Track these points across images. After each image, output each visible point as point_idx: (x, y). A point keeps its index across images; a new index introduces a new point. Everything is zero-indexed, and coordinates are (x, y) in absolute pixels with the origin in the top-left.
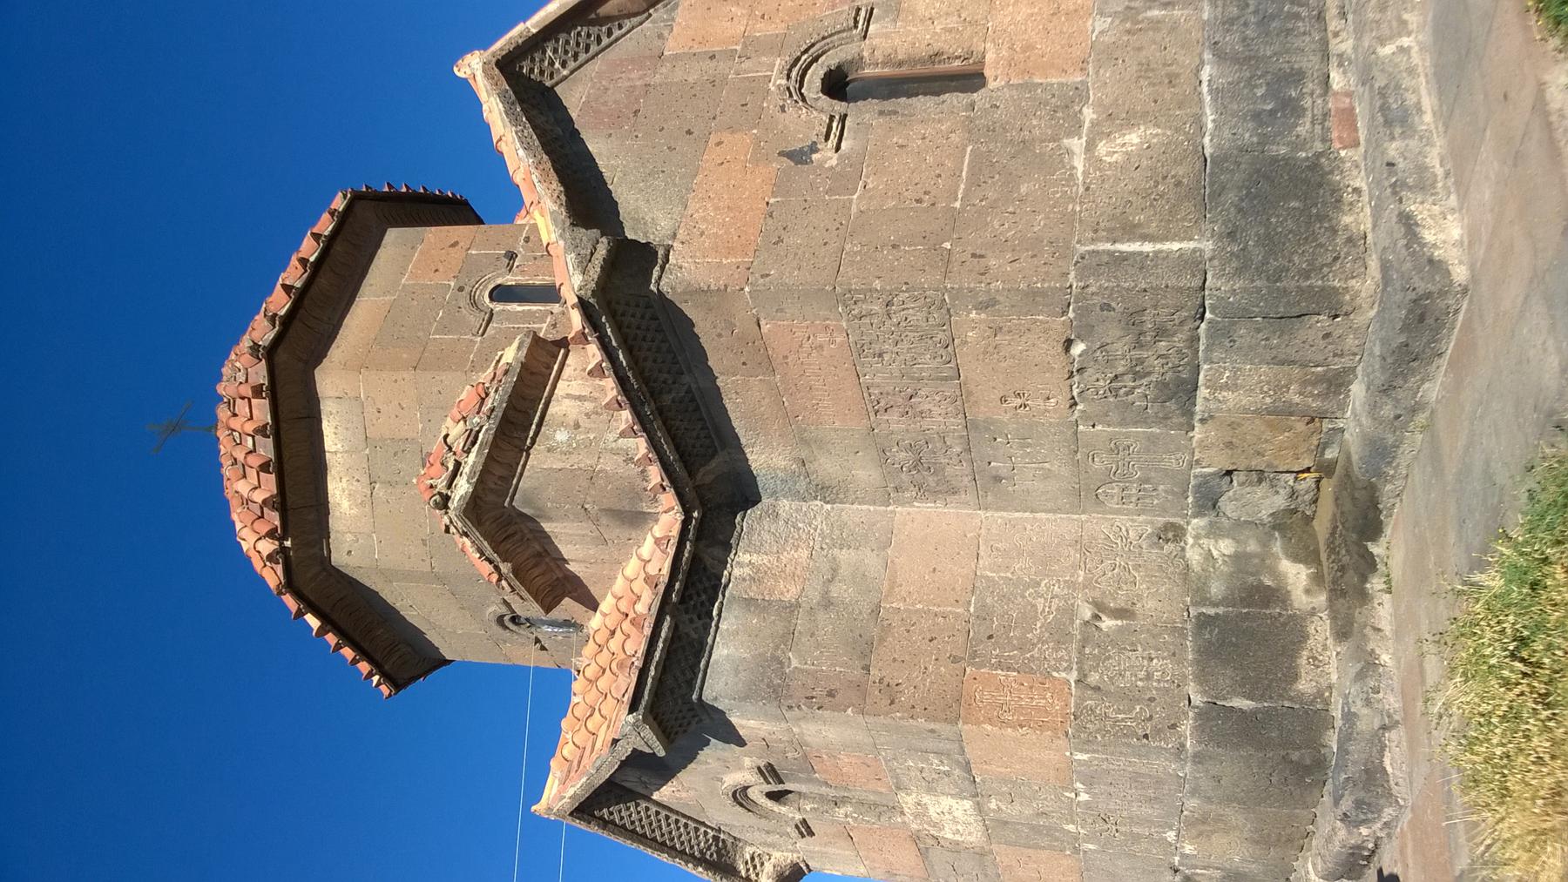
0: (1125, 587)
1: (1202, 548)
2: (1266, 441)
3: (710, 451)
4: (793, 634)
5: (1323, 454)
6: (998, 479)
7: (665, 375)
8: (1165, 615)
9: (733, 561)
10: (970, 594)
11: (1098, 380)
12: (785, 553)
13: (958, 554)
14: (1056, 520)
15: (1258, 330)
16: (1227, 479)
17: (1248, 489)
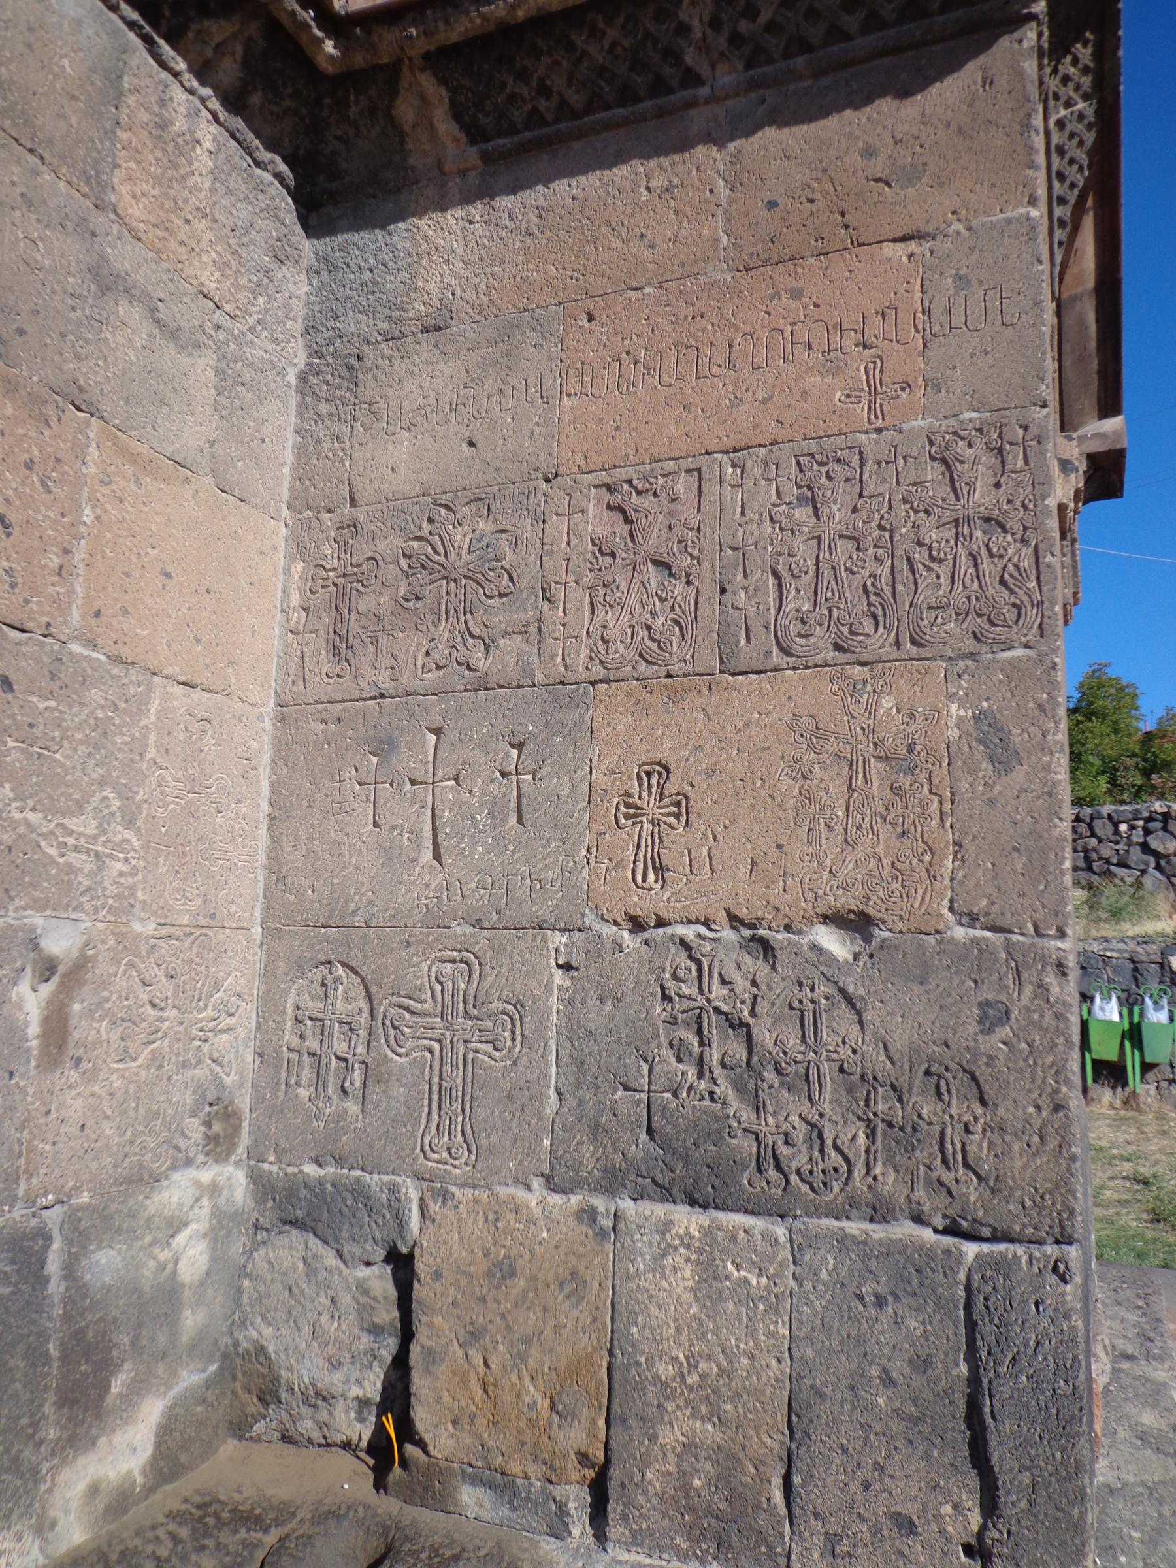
0: (115, 1036)
1: (192, 1207)
2: (523, 1357)
3: (486, 121)
4: (31, 151)
5: (475, 1481)
6: (383, 748)
7: (764, 17)
8: (48, 1147)
9: (203, 100)
10: (112, 649)
11: (724, 982)
12: (210, 235)
13: (198, 640)
14: (253, 869)
15: (921, 1364)
16: (382, 1253)
17: (346, 1301)
